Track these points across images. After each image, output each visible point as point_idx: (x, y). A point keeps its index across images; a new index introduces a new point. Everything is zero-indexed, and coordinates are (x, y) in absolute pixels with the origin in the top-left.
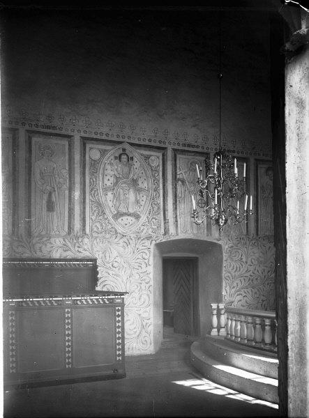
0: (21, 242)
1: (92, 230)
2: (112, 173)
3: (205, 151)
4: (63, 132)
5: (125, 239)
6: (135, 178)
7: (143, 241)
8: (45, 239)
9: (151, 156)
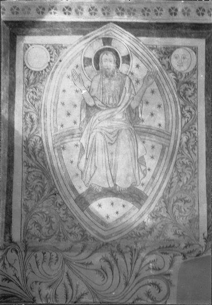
1: (26, 232)
9: (175, 48)
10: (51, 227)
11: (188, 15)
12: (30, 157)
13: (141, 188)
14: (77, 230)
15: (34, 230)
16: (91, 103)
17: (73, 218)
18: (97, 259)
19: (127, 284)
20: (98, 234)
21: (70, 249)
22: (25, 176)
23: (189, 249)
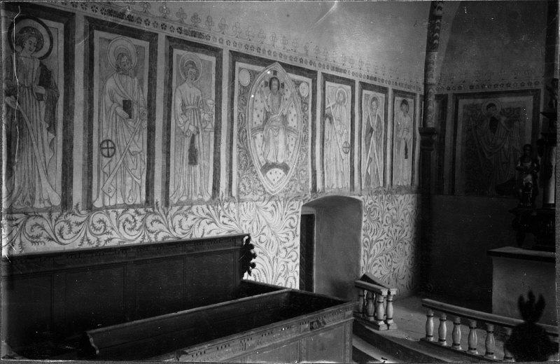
0: (155, 214)
1: (239, 190)
4: (211, 43)
5: (273, 202)
6: (284, 114)
7: (292, 203)
8: (186, 207)
9: (302, 82)
14: (261, 189)
18: (269, 205)
21: (258, 200)
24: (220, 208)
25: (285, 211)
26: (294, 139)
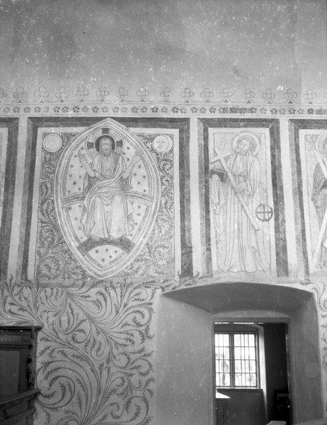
1: (38, 272)
2: (83, 172)
3: (269, 115)
6: (125, 177)
10: (58, 269)
11: (166, 112)
12: (43, 215)
13: (130, 238)
15: (45, 271)
16: (92, 175)
17: (75, 261)
19: (117, 312)
20: (95, 273)
21: (72, 286)
22: (39, 229)
23: (167, 284)
24: (6, 293)
25: (125, 301)
26: (143, 207)
